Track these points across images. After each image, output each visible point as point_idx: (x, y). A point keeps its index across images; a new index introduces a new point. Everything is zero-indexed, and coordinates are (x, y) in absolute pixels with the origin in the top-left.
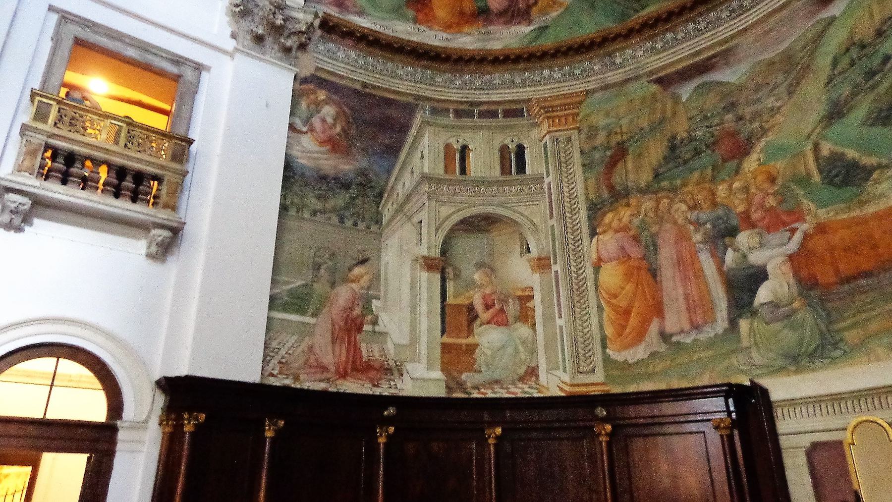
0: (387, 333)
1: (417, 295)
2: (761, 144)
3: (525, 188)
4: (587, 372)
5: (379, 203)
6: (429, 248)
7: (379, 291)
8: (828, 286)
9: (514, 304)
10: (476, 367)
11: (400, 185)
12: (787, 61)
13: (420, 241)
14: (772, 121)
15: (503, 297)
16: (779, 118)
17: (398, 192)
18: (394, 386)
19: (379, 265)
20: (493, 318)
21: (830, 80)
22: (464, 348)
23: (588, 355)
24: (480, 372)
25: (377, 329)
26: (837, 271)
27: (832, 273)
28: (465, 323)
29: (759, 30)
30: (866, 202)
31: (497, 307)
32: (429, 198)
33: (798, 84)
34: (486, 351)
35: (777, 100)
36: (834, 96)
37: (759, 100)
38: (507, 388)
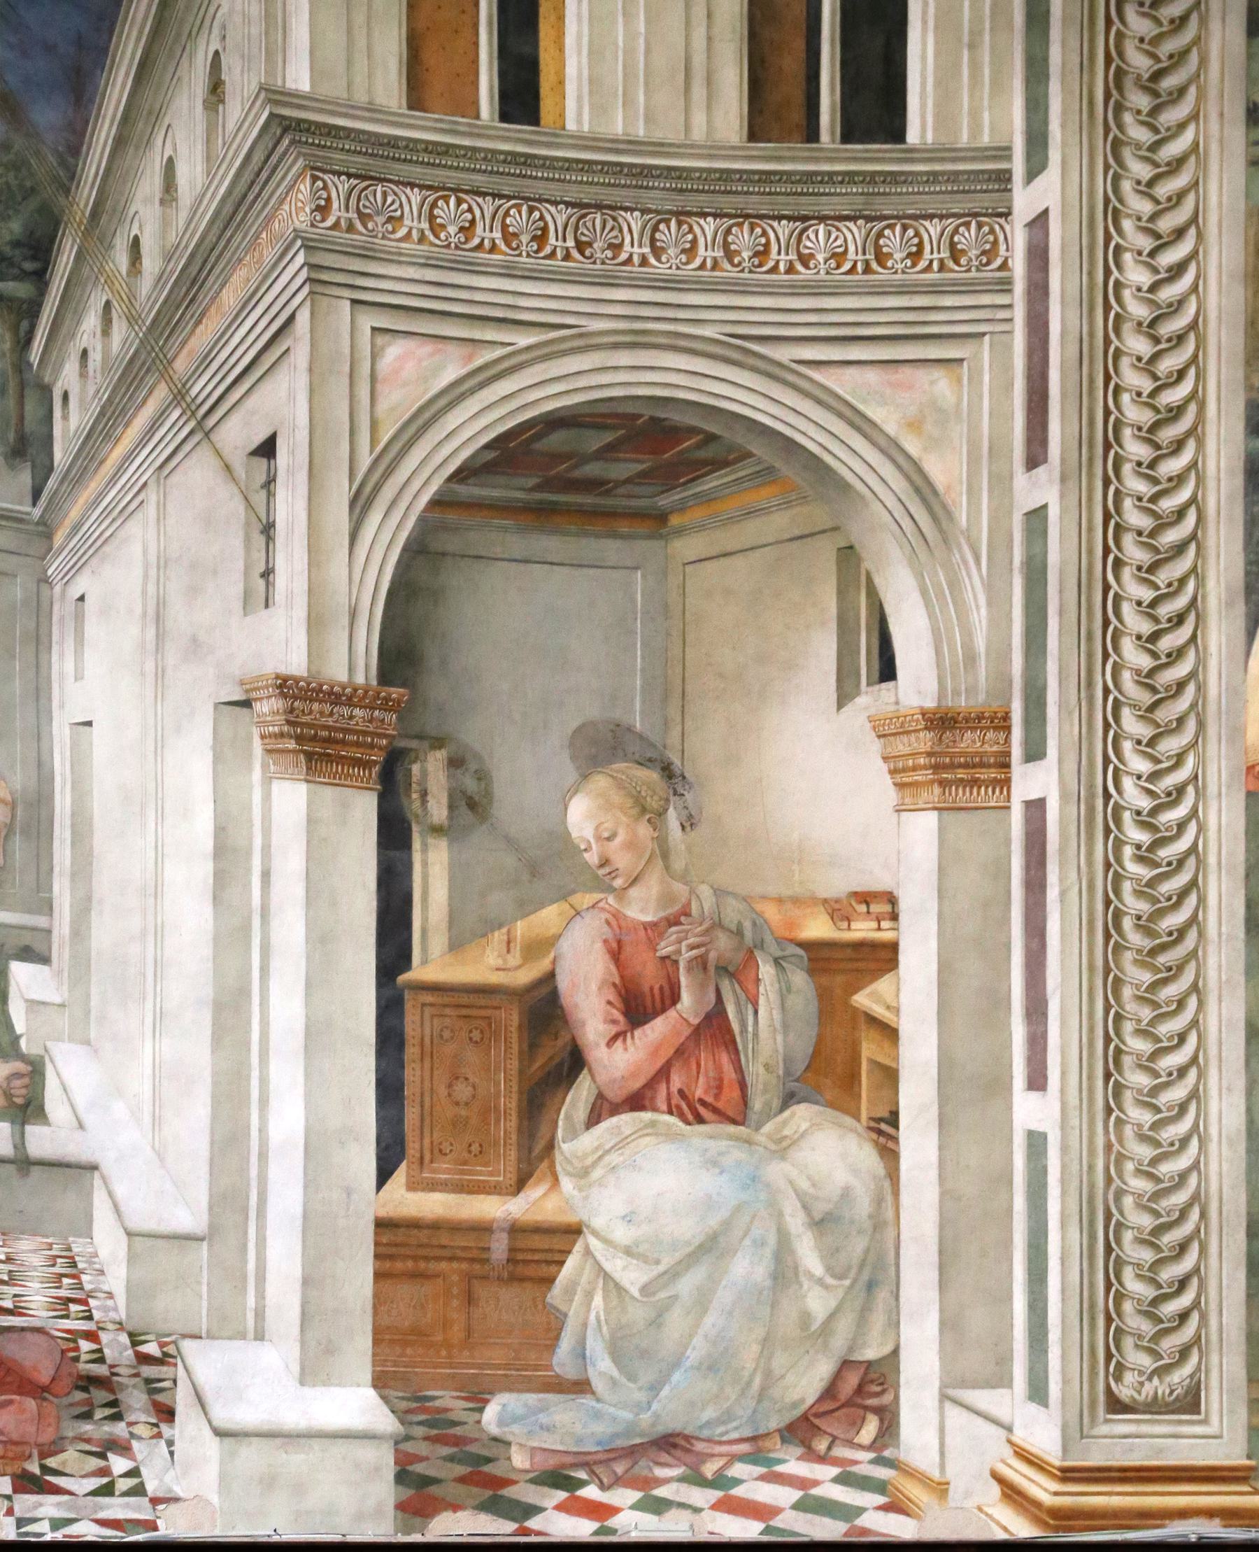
0: (94, 1168)
1: (246, 928)
3: (893, 241)
4: (1155, 1407)
5: (32, 310)
6: (316, 623)
7: (47, 907)
9: (785, 992)
10: (562, 1360)
11: (149, 184)
13: (268, 574)
15: (723, 942)
17: (135, 231)
18: (130, 1482)
19: (39, 734)
20: (663, 1073)
22: (499, 1247)
23: (1171, 1308)
24: (581, 1386)
25: (40, 1141)
28: (509, 1102)
31: (689, 1004)
32: (317, 282)
34: (616, 1266)
38: (719, 1482)
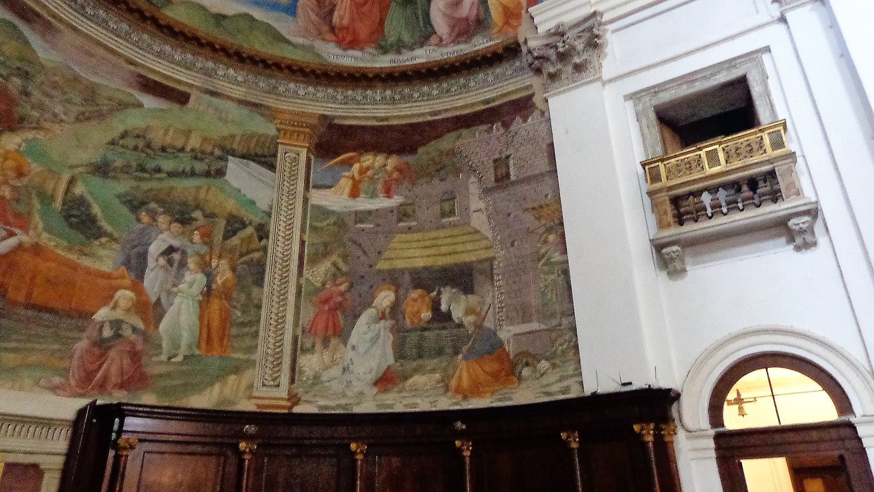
2: (30, 135)
8: (15, 304)
12: (91, 94)
14: (47, 125)
16: (57, 128)
21: (113, 143)
26: (29, 295)
27: (24, 292)
29: (80, 41)
30: (86, 255)
33: (88, 119)
35: (65, 114)
36: (110, 156)
37: (48, 95)
